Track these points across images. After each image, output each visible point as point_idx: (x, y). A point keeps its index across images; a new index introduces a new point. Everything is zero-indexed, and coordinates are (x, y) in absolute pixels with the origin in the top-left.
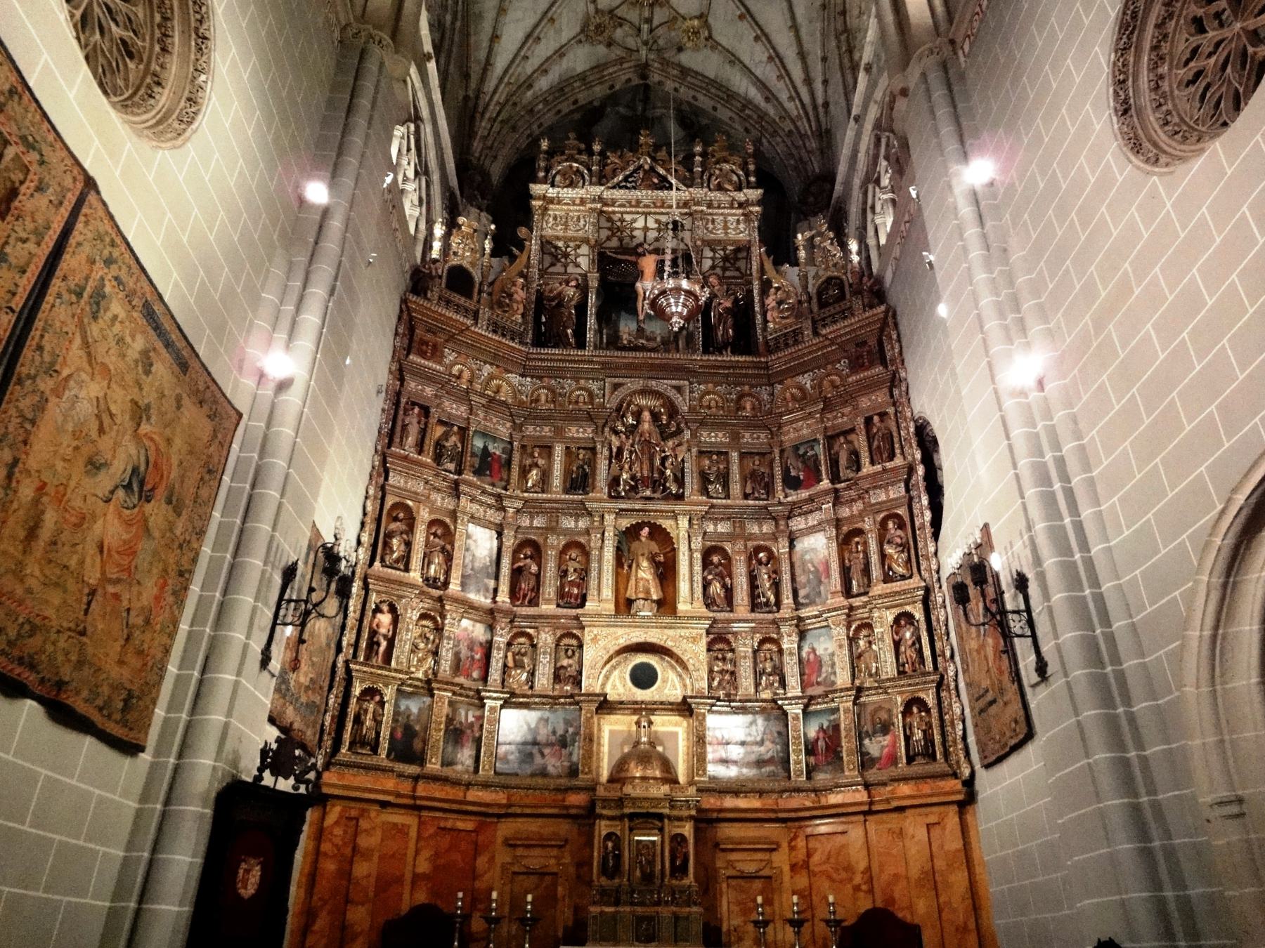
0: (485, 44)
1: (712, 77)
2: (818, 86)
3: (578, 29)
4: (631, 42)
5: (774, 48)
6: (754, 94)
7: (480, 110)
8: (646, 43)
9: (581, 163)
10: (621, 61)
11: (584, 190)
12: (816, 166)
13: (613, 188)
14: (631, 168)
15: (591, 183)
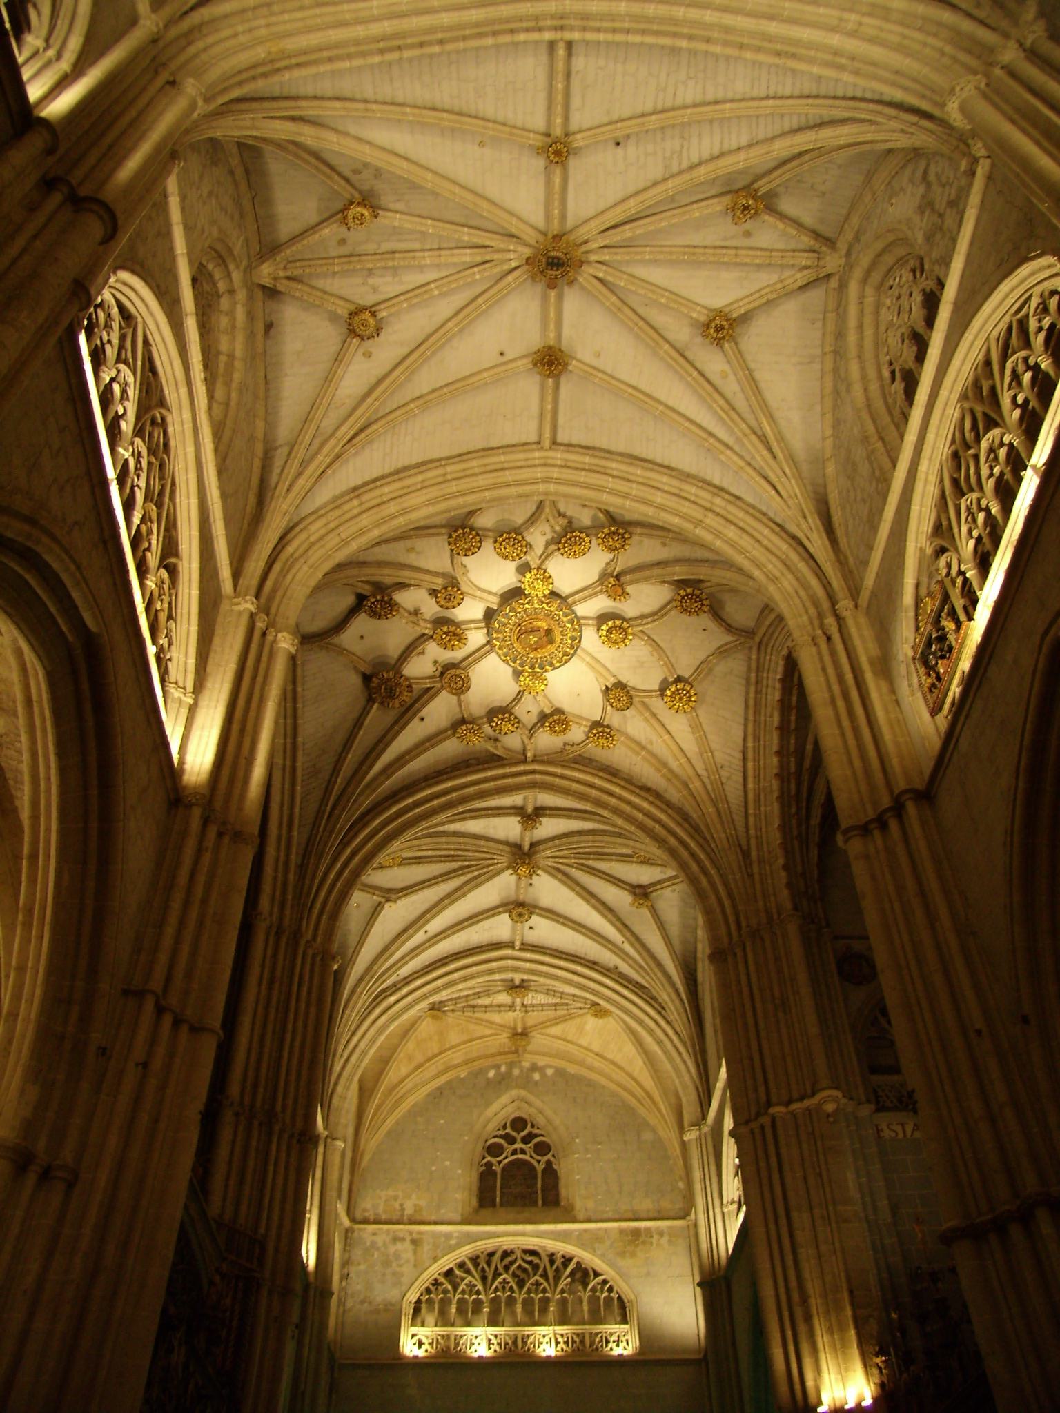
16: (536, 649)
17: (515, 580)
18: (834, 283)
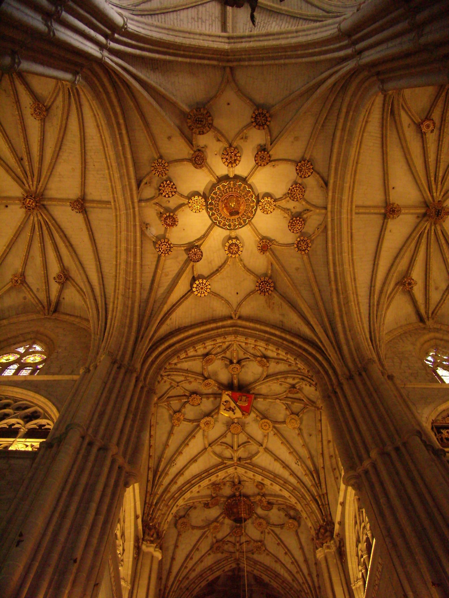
1: (268, 565)
3: (209, 548)
4: (232, 550)
5: (293, 557)
6: (286, 575)
8: (238, 550)
10: (226, 559)
16: (226, 206)
17: (259, 192)
18: (421, 324)
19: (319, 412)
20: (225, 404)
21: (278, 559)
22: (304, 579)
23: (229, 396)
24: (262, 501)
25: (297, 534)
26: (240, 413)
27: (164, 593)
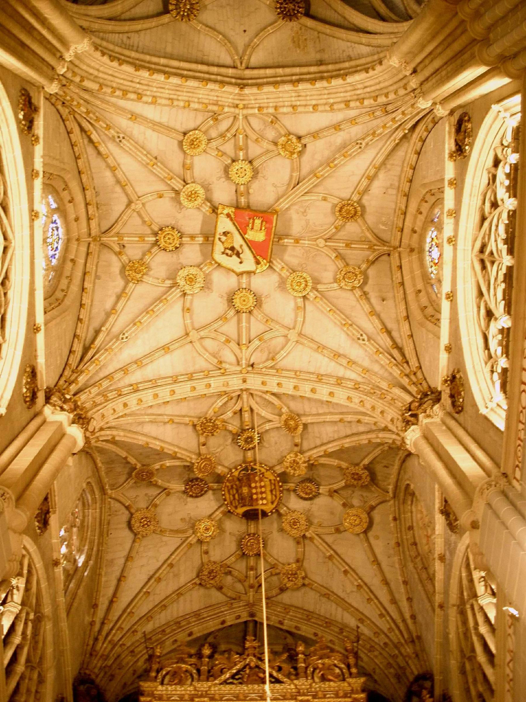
0: (114, 583)
2: (404, 604)
3: (194, 575)
5: (361, 579)
7: (104, 633)
9: (191, 665)
11: (192, 688)
12: (414, 669)
13: (221, 684)
14: (238, 667)
15: (199, 680)
19: (397, 255)
20: (224, 238)
21: (333, 592)
22: (382, 609)
23: (231, 220)
24: (298, 463)
25: (367, 540)
26: (252, 260)
27: (100, 631)
